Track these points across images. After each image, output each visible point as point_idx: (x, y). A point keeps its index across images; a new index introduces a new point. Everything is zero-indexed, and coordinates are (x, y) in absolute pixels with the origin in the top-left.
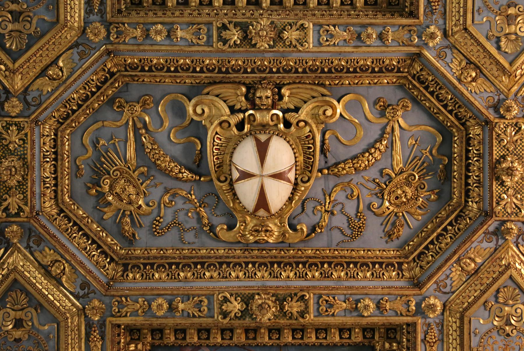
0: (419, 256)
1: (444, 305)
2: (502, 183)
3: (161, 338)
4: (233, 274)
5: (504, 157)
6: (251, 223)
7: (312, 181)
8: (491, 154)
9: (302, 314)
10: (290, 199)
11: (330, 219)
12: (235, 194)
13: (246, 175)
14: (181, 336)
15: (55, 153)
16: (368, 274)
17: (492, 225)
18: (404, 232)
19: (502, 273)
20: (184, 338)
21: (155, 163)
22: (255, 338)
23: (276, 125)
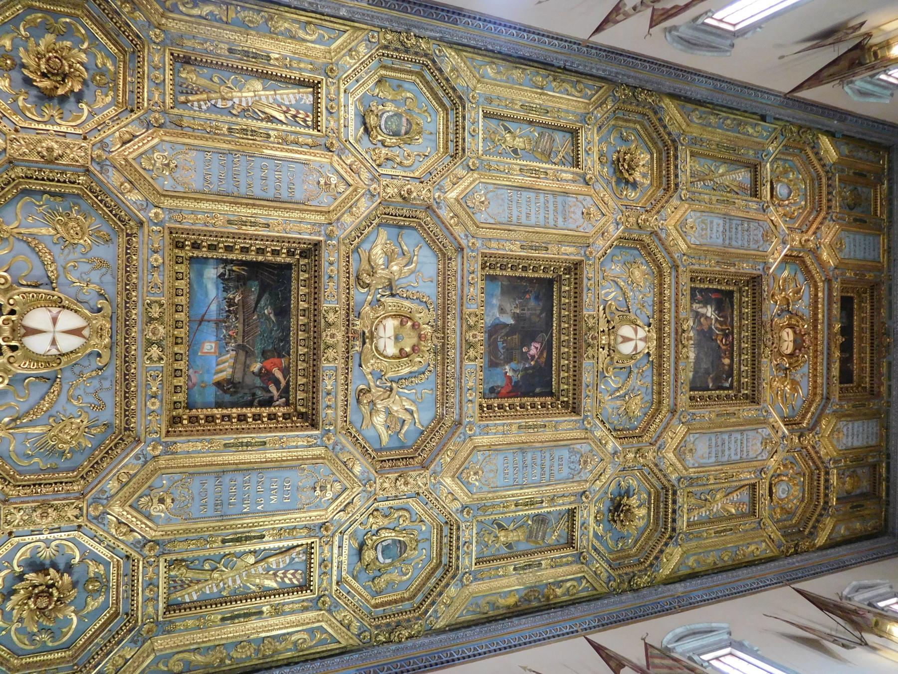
0: (121, 221)
1: (156, 207)
2: (61, 156)
3: (180, 402)
4: (133, 352)
5: (39, 153)
6: (95, 341)
7: (61, 295)
8: (37, 162)
9: (161, 305)
10: (76, 311)
11: (93, 283)
12: (72, 352)
13: (54, 342)
14: (179, 390)
15: (34, 485)
16: (134, 257)
17: (95, 168)
18: (105, 230)
19: (131, 165)
20: (181, 387)
21: (45, 412)
22: (182, 338)
23: (13, 321)
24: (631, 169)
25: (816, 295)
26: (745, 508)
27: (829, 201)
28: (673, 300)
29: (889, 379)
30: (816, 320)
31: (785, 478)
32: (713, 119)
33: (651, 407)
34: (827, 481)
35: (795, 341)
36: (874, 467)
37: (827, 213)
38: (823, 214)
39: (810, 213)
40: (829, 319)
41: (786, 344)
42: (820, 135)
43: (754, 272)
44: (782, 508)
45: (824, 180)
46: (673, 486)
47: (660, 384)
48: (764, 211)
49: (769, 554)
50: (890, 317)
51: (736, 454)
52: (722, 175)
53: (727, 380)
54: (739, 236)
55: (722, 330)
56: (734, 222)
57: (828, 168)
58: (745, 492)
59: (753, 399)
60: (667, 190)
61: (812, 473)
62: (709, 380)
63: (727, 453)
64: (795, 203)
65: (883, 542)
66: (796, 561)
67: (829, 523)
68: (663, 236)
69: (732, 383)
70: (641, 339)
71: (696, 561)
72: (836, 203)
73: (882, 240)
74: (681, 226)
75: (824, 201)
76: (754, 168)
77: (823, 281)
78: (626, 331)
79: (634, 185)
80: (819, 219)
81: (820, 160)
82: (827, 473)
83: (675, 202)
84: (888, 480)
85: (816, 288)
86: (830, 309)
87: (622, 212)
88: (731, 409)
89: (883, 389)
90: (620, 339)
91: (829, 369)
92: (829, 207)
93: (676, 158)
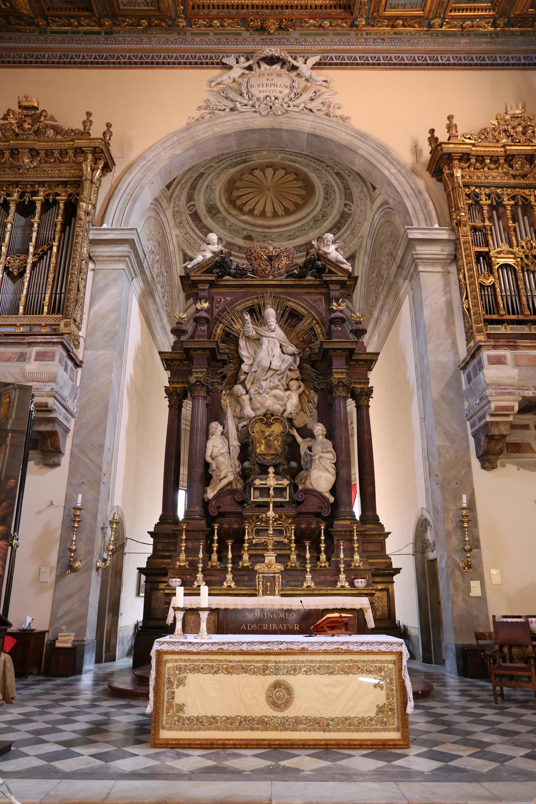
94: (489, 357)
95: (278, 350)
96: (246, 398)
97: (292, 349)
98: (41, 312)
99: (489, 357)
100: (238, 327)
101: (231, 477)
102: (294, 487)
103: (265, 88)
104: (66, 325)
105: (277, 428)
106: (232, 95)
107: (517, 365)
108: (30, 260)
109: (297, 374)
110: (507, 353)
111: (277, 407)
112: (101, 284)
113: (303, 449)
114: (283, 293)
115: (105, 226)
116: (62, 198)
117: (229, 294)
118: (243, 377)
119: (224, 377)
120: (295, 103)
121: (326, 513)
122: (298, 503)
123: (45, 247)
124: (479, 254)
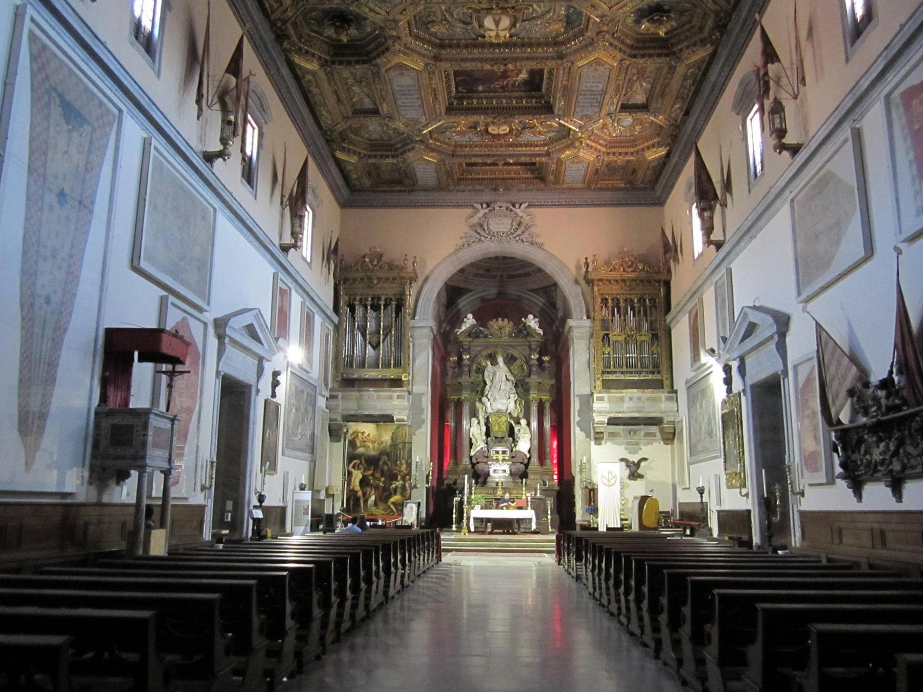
24: (652, 21)
25: (537, 146)
26: (358, 107)
27: (614, 154)
28: (533, 55)
29: (470, 191)
30: (516, 146)
31: (385, 129)
32: (690, 81)
33: (437, 38)
34: (387, 157)
35: (499, 135)
36: (400, 182)
37: (604, 153)
38: (604, 149)
39: (605, 140)
40: (517, 155)
41: (497, 129)
42: (667, 148)
43: (556, 110)
44: (360, 128)
45: (632, 150)
46: (371, 61)
47: (458, 46)
48: (608, 114)
49: (322, 120)
50: (520, 191)
51: (402, 103)
52: (641, 85)
53: (464, 89)
54: (587, 100)
55: (507, 85)
56: (599, 97)
57: (641, 153)
58: (372, 106)
59: (450, 110)
60: (632, 47)
61: (391, 146)
62: (463, 77)
63: (403, 97)
64: (615, 130)
65: (345, 191)
66: (321, 142)
67: (353, 159)
68: (590, 49)
69: (462, 92)
70: (497, 33)
71: (309, 81)
72: (612, 158)
73: (581, 185)
74: (598, 62)
75: (614, 150)
76: (644, 107)
77: (548, 150)
78: (505, 22)
79: (638, 22)
80: (599, 147)
81: (648, 148)
82: (393, 157)
83: (619, 56)
84: (392, 191)
85: (544, 145)
86: (525, 155)
87: (613, 20)
88: (440, 98)
89: (462, 187)
90: (497, 18)
91: (476, 156)
92: (608, 154)
93: (659, 55)
94: (597, 397)
95: (504, 378)
96: (488, 404)
97: (511, 377)
98: (390, 366)
99: (597, 397)
100: (484, 364)
101: (482, 446)
102: (512, 451)
103: (497, 226)
104: (405, 377)
105: (504, 419)
106: (479, 230)
107: (609, 401)
108: (382, 339)
109: (514, 391)
110: (605, 395)
111: (504, 408)
112: (417, 350)
113: (516, 429)
114: (507, 345)
115: (417, 318)
116: (394, 303)
117: (479, 346)
118: (486, 393)
119: (477, 392)
120: (514, 235)
121: (526, 461)
122: (513, 457)
123: (388, 330)
124: (606, 334)
